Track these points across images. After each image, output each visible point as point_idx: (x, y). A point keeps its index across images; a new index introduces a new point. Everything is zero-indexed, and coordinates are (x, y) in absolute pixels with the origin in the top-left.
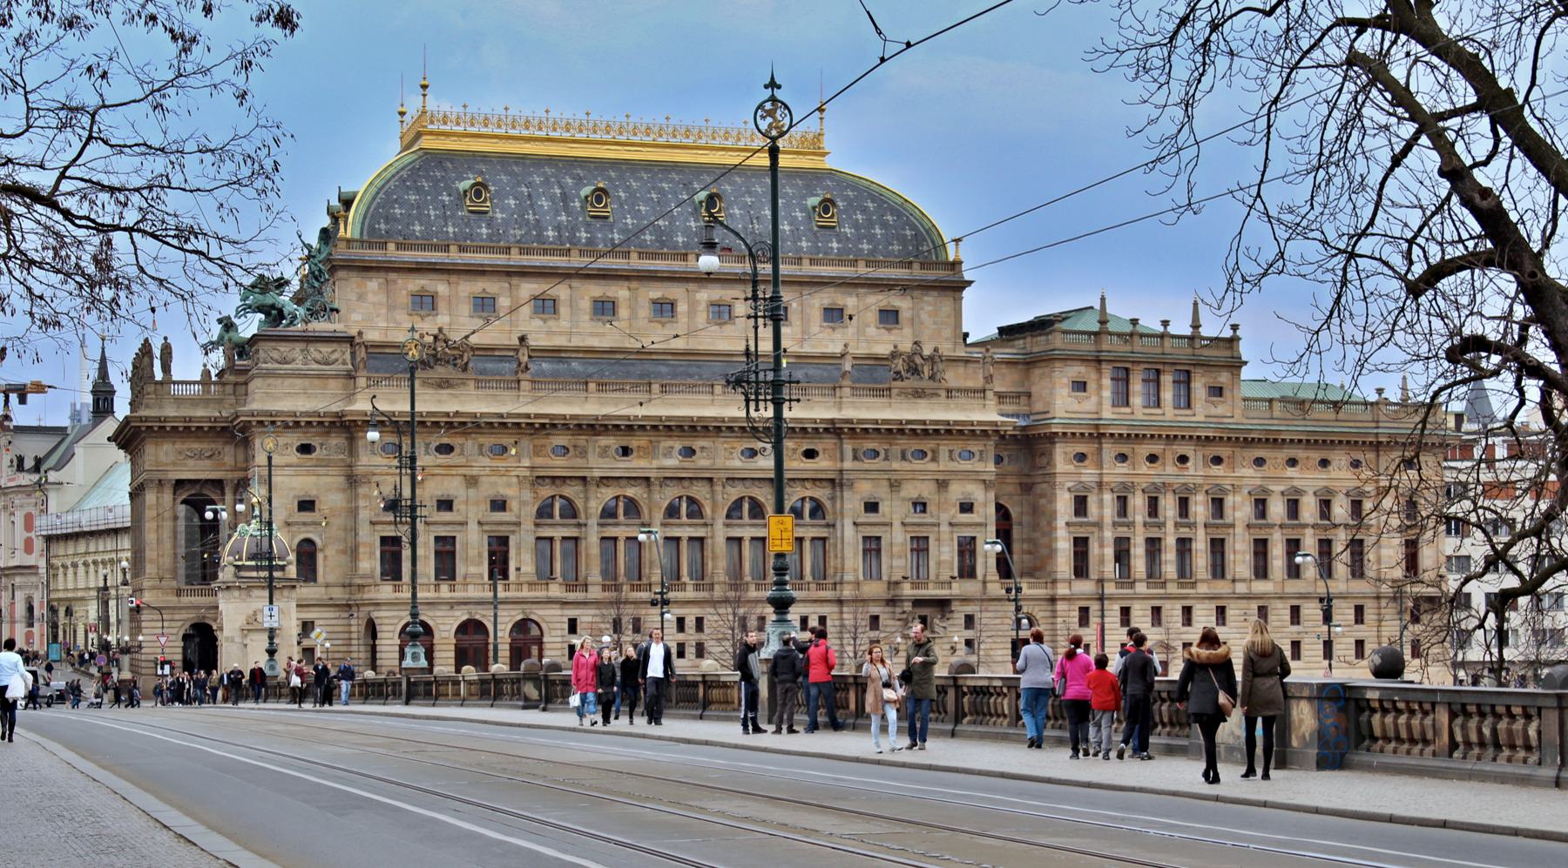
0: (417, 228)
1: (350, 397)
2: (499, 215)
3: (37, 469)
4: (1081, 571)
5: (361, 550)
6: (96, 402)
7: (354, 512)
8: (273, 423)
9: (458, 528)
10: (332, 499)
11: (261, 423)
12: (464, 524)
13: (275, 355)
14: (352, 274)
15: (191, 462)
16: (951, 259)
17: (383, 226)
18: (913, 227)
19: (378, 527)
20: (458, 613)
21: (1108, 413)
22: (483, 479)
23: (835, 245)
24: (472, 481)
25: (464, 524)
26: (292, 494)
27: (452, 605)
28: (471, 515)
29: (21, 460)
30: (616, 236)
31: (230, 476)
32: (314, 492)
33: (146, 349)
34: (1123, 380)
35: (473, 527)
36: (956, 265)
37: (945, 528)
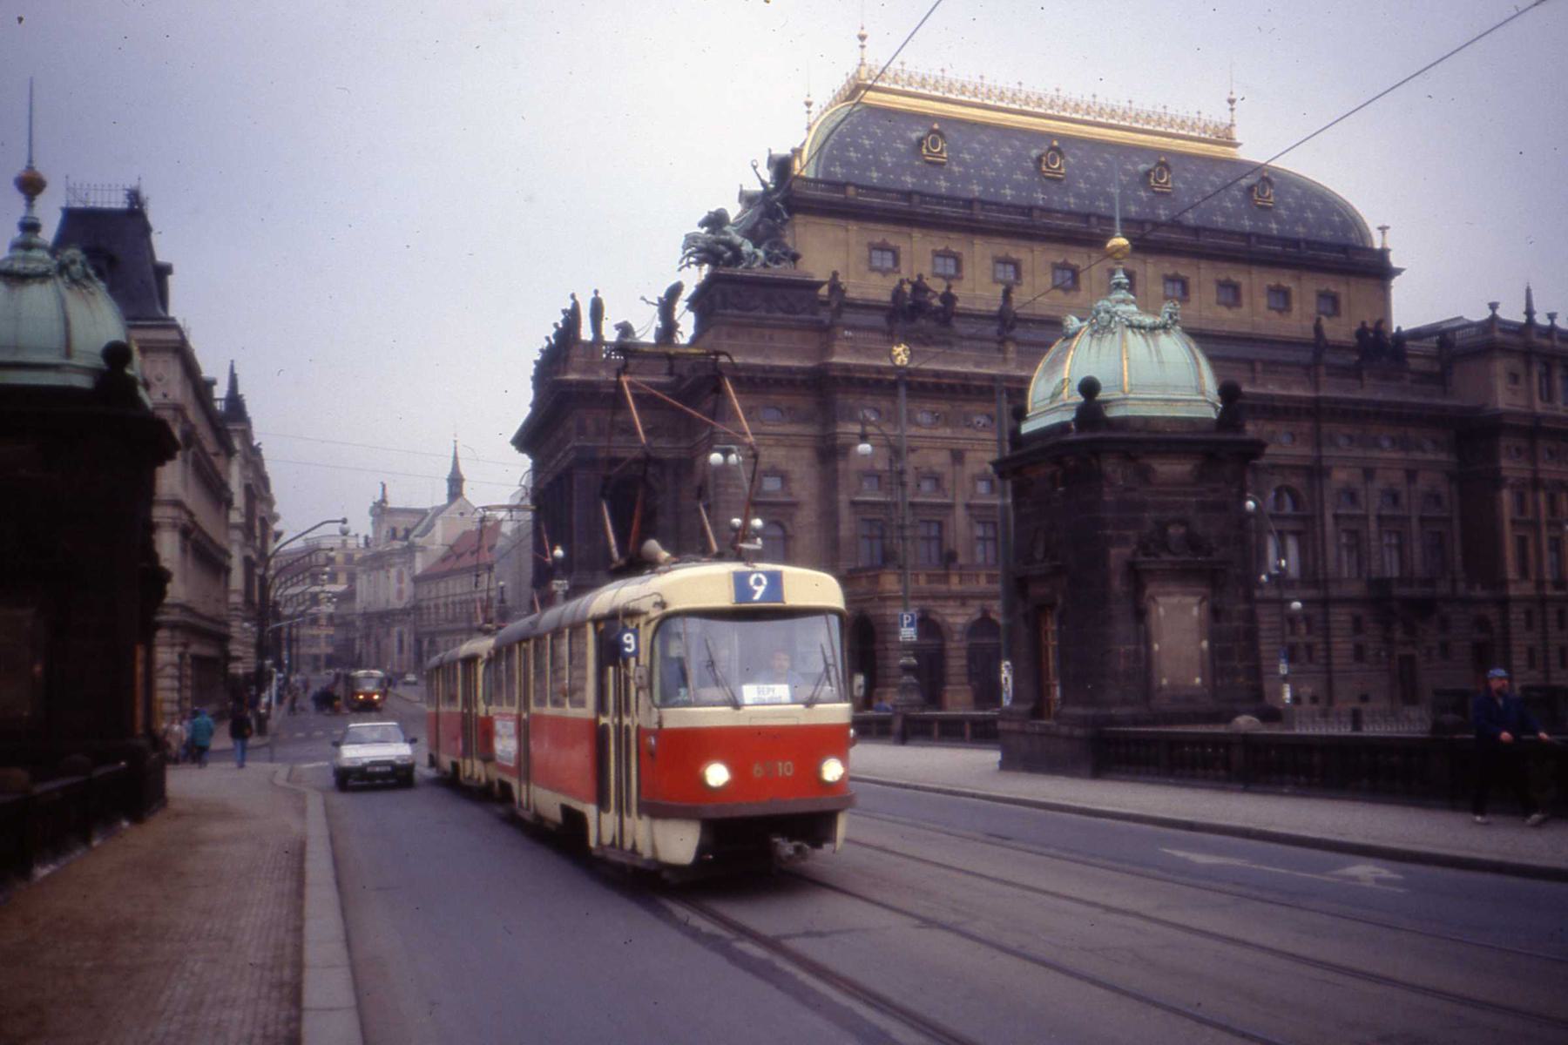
0: (875, 175)
1: (827, 349)
2: (956, 169)
3: (406, 537)
4: (1523, 571)
6: (451, 487)
12: (950, 507)
16: (1377, 246)
17: (838, 169)
18: (1340, 214)
20: (970, 611)
21: (1539, 407)
23: (1274, 226)
25: (950, 507)
27: (963, 599)
29: (394, 531)
30: (1072, 200)
34: (1547, 375)
35: (960, 512)
36: (1383, 253)
37: (1415, 522)
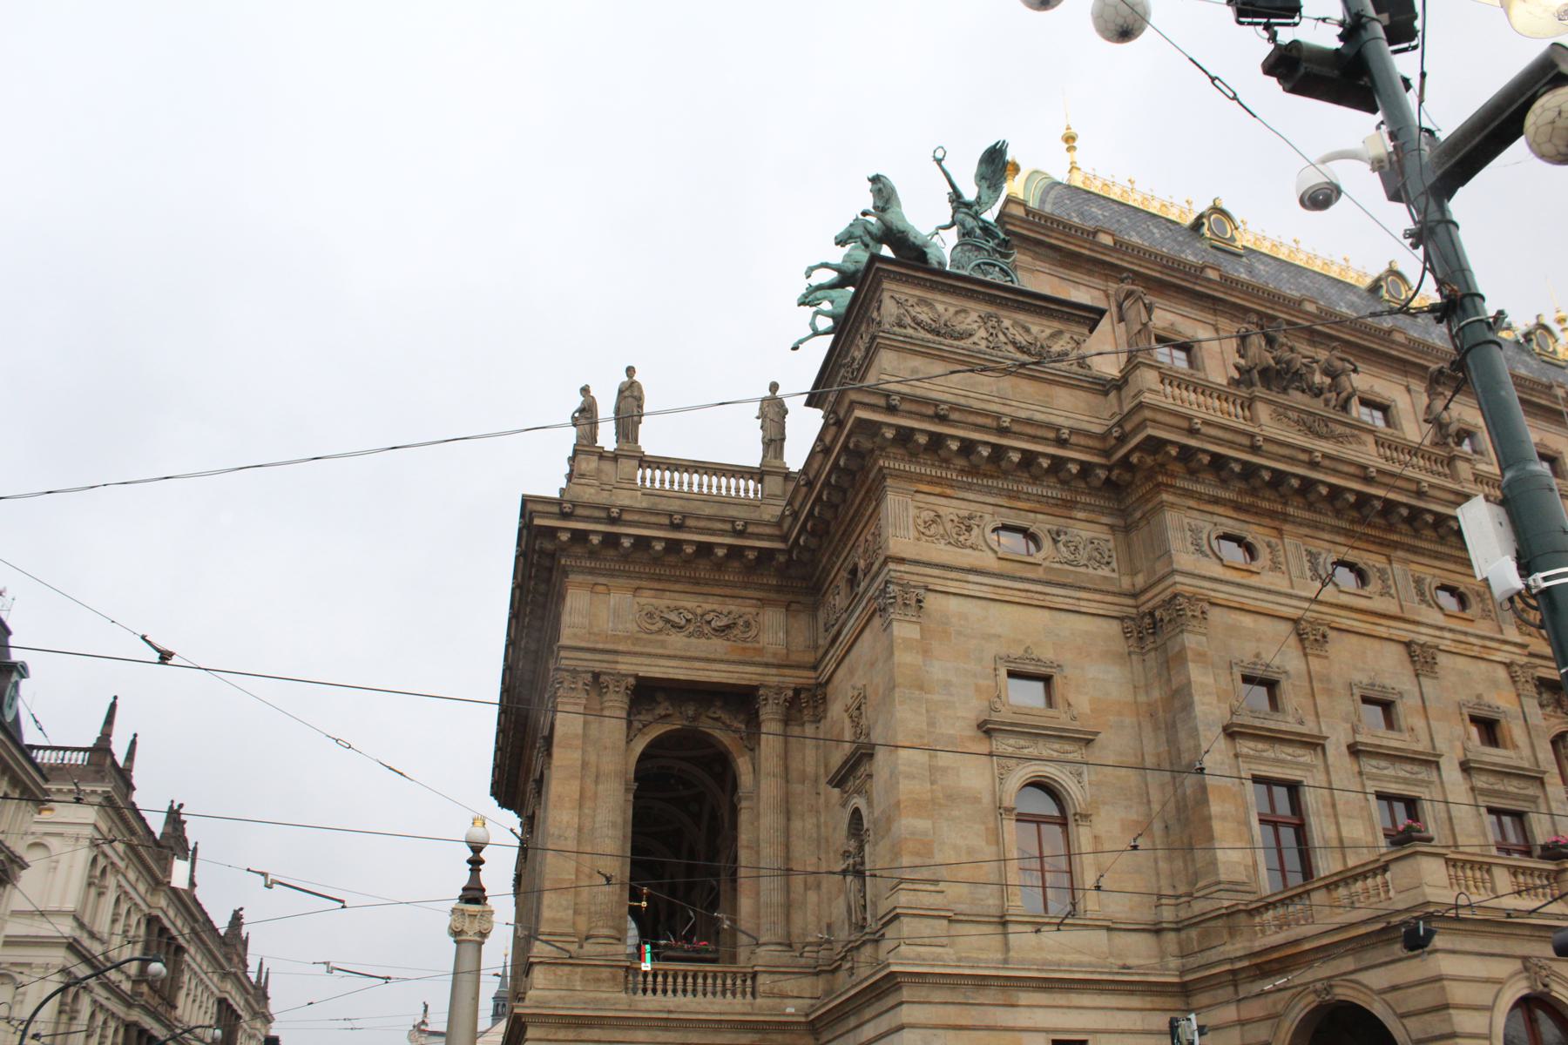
5: (1215, 808)
7: (1178, 701)
8: (937, 441)
9: (1423, 774)
10: (1100, 681)
11: (905, 437)
13: (924, 315)
14: (1039, 265)
15: (677, 641)
19: (1246, 747)
22: (1442, 659)
24: (1421, 658)
26: (993, 648)
28: (1441, 746)
31: (773, 678)
32: (1048, 654)
33: (586, 415)
